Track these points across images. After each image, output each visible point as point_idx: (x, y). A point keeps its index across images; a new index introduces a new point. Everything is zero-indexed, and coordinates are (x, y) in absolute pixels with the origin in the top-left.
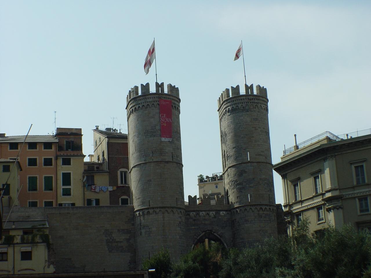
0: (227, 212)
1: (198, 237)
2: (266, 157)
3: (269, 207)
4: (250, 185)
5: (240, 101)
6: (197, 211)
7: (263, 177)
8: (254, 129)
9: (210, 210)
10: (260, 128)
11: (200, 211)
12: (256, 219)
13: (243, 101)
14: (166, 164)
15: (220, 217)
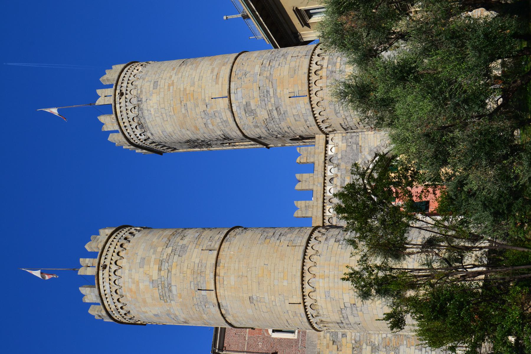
0: (330, 142)
2: (224, 65)
3: (316, 56)
5: (124, 113)
6: (324, 203)
7: (257, 69)
8: (171, 87)
9: (325, 176)
10: (171, 77)
11: (324, 196)
13: (123, 109)
14: (221, 264)
15: (339, 156)
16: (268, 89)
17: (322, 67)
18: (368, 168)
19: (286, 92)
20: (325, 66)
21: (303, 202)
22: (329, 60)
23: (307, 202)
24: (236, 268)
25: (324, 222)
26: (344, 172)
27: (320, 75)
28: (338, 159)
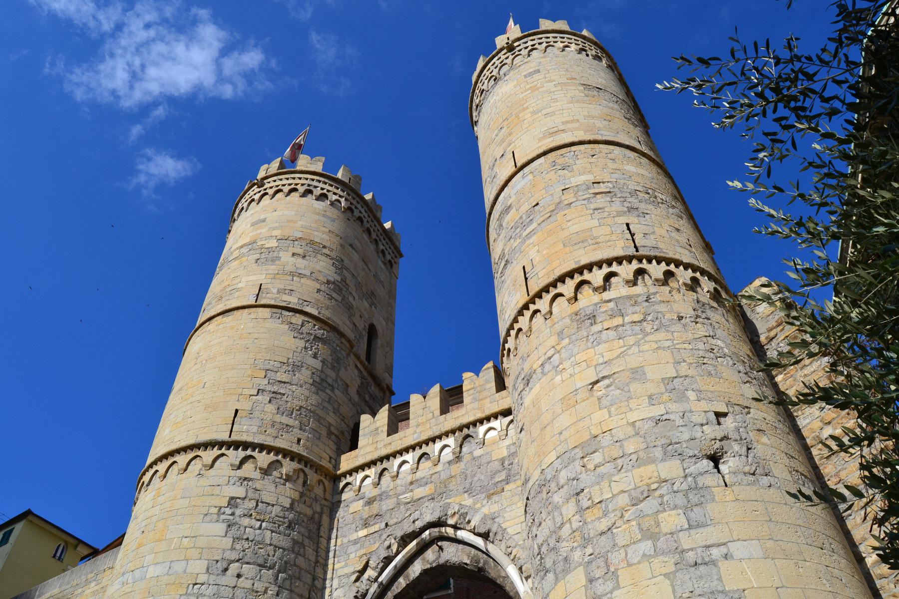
1: (380, 574)
4: (525, 234)
6: (381, 459)
11: (394, 455)
12: (567, 341)
15: (478, 452)
16: (535, 220)
17: (605, 288)
18: (456, 527)
19: (533, 253)
20: (606, 295)
21: (386, 421)
22: (629, 297)
23: (386, 428)
24: (212, 343)
25: (344, 475)
26: (443, 476)
27: (579, 296)
28: (471, 453)
